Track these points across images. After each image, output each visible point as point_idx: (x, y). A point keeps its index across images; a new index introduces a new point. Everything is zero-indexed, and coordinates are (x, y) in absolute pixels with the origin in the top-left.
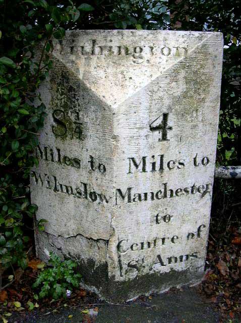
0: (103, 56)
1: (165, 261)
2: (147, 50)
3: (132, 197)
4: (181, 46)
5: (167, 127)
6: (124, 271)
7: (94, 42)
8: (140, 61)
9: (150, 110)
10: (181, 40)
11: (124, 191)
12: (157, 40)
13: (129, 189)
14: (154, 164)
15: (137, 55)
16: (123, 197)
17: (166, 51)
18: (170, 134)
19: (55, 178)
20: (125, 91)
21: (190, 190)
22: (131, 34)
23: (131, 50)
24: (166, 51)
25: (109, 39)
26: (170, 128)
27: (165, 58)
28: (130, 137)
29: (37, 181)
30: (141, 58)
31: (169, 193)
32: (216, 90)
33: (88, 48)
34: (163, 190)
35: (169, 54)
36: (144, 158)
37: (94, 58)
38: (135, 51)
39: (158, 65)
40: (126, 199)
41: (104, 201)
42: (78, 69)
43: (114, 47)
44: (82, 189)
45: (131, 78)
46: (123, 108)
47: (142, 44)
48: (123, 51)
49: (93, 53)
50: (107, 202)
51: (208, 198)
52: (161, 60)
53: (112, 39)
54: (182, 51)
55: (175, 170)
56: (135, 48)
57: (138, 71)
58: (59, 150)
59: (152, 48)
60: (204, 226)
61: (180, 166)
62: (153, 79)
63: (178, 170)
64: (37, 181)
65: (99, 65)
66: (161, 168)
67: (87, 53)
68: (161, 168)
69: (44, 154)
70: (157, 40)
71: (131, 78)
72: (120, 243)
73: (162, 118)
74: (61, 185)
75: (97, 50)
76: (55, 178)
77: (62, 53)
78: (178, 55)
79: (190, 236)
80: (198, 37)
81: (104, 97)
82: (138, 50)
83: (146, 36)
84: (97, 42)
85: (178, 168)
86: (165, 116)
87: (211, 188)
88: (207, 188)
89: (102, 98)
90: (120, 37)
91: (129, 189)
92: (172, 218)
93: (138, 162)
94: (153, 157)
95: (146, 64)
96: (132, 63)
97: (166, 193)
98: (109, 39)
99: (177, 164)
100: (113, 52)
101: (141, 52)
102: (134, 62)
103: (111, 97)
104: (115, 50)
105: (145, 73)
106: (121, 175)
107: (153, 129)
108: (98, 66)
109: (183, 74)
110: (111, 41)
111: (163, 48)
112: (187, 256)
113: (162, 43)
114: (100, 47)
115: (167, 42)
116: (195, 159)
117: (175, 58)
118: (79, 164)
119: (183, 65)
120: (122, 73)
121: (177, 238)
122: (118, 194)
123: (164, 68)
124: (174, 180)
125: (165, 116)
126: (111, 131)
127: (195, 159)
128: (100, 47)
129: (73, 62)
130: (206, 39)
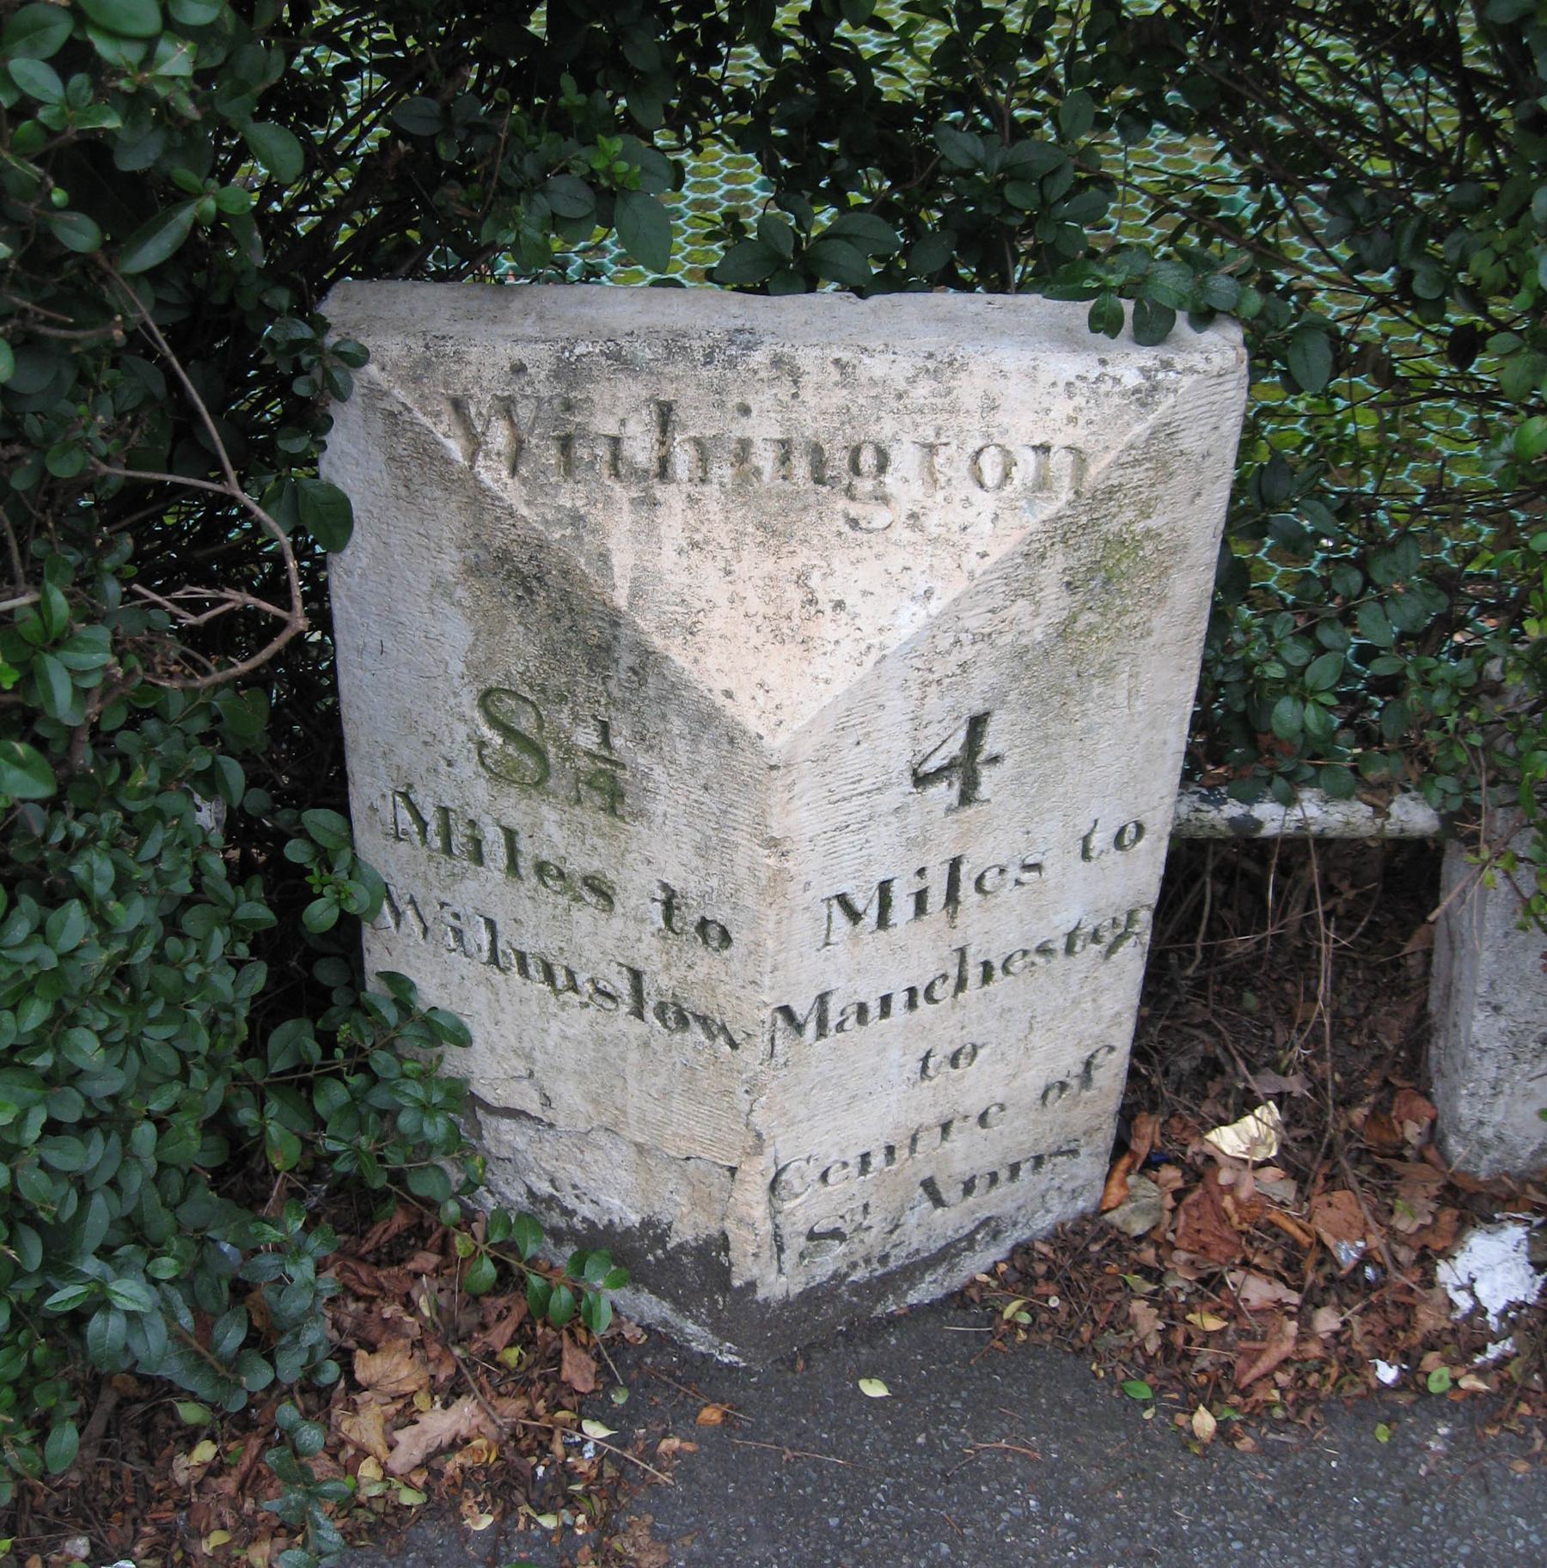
0: (712, 490)
1: (951, 1193)
2: (905, 458)
3: (833, 1019)
4: (1058, 441)
5: (981, 758)
6: (789, 1257)
7: (665, 416)
8: (879, 516)
9: (918, 723)
10: (1062, 407)
11: (803, 1007)
12: (953, 411)
13: (822, 999)
14: (921, 898)
15: (865, 485)
16: (799, 1028)
17: (991, 468)
18: (989, 780)
19: (491, 924)
20: (820, 667)
21: (1060, 945)
22: (835, 375)
23: (839, 461)
24: (991, 468)
25: (733, 400)
26: (995, 760)
27: (986, 502)
28: (837, 822)
29: (398, 915)
30: (884, 499)
31: (974, 973)
32: (1192, 585)
33: (641, 448)
34: (954, 972)
35: (1007, 476)
36: (885, 887)
37: (671, 496)
38: (855, 469)
39: (956, 538)
40: (811, 1029)
41: (721, 1040)
42: (604, 557)
43: (759, 445)
44: (623, 986)
45: (839, 605)
46: (807, 748)
47: (885, 429)
48: (801, 467)
49: (664, 470)
50: (734, 1045)
51: (1132, 962)
52: (969, 516)
53: (750, 401)
54: (1060, 461)
55: (1008, 894)
56: (856, 452)
57: (868, 575)
58: (510, 835)
59: (931, 449)
60: (1112, 1049)
61: (1026, 876)
62: (935, 606)
63: (1019, 890)
64: (398, 915)
65: (698, 537)
66: (952, 897)
67: (641, 475)
68: (952, 897)
69: (433, 827)
70: (953, 411)
71: (839, 605)
72: (778, 1174)
73: (961, 735)
74: (521, 957)
75: (683, 459)
76: (491, 924)
77: (523, 470)
78: (1042, 484)
79: (1053, 1094)
80: (1136, 391)
81: (728, 694)
82: (868, 459)
83: (902, 385)
84: (680, 414)
85: (1018, 882)
86: (977, 724)
87: (1145, 916)
88: (1131, 916)
89: (720, 700)
90: (784, 390)
91: (822, 999)
92: (982, 1053)
93: (859, 906)
94: (921, 872)
95: (907, 535)
96: (846, 529)
97: (970, 973)
98: (733, 400)
99: (1014, 872)
100: (758, 472)
101: (882, 467)
102: (854, 523)
103: (760, 694)
104: (765, 459)
105: (905, 580)
106: (800, 957)
107: (921, 780)
108: (694, 545)
109: (1058, 561)
110: (745, 410)
111: (979, 452)
112: (1039, 1161)
113: (974, 424)
114: (697, 442)
115: (1001, 418)
116: (1086, 840)
117: (1030, 502)
118: (609, 899)
119: (1063, 532)
120: (801, 579)
121: (1002, 1107)
122: (780, 1023)
123: (984, 555)
124: (991, 927)
125: (977, 724)
126: (760, 821)
127: (1086, 840)
128: (697, 442)
129: (577, 519)
130: (1171, 399)
